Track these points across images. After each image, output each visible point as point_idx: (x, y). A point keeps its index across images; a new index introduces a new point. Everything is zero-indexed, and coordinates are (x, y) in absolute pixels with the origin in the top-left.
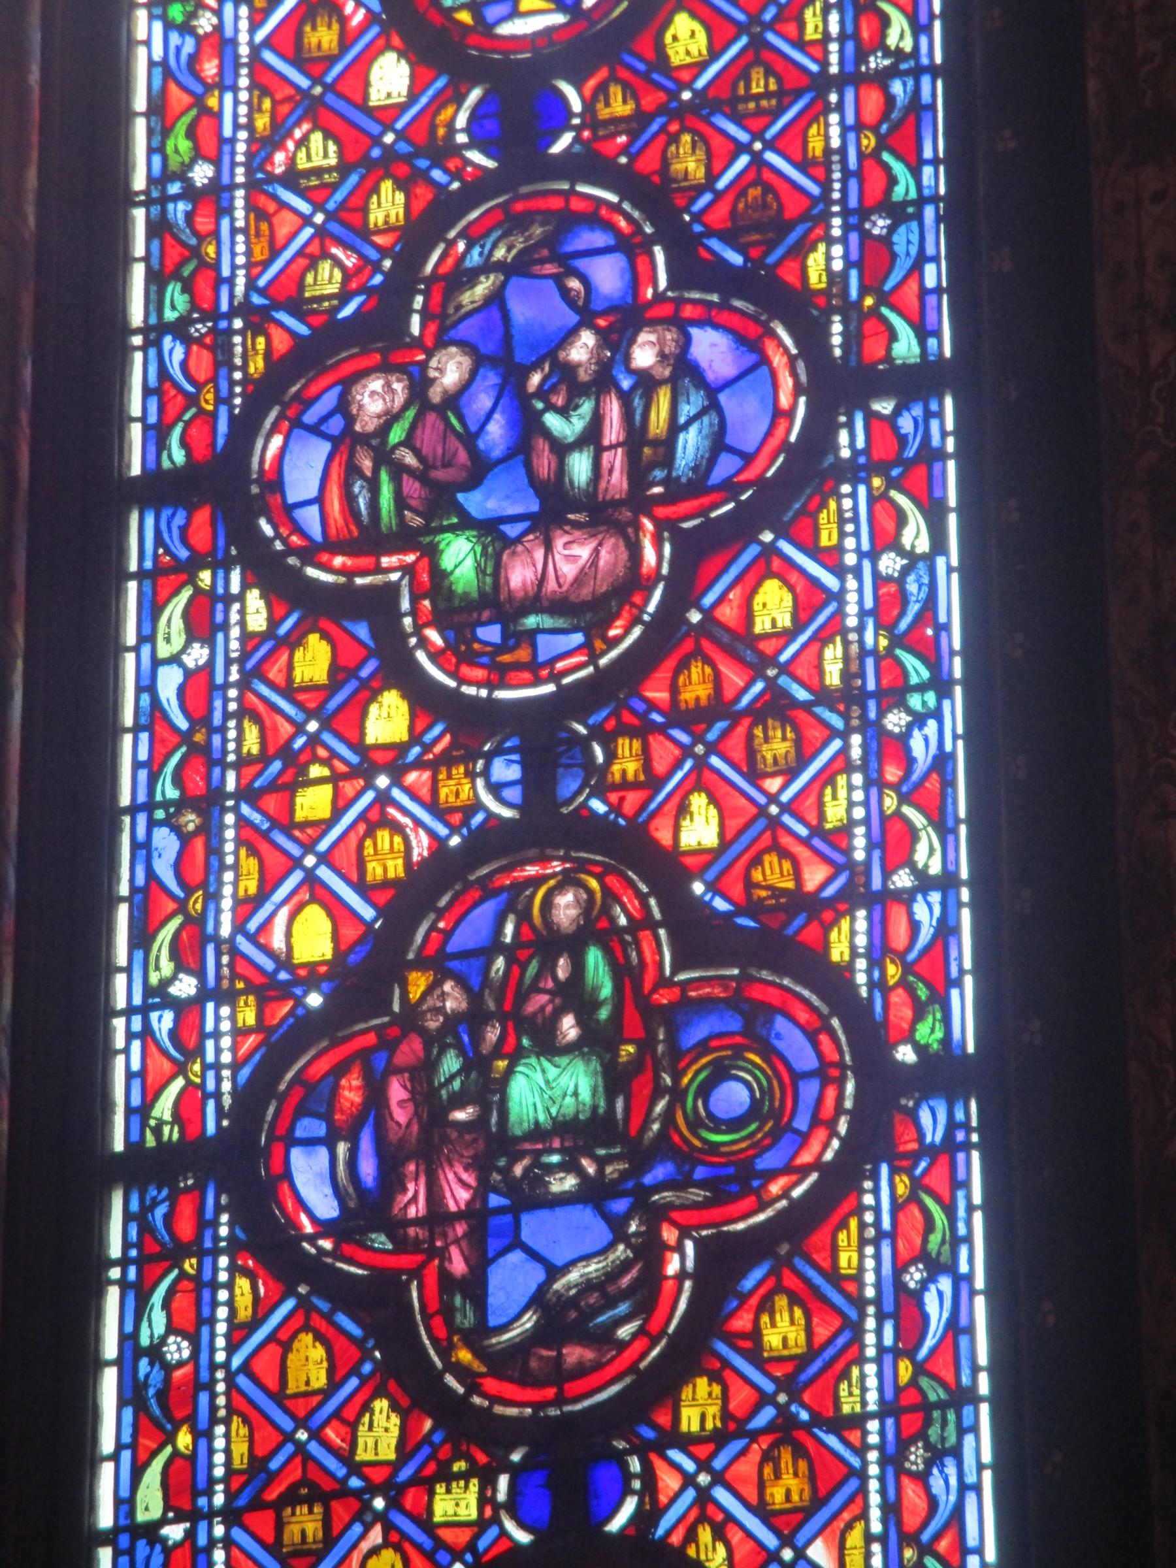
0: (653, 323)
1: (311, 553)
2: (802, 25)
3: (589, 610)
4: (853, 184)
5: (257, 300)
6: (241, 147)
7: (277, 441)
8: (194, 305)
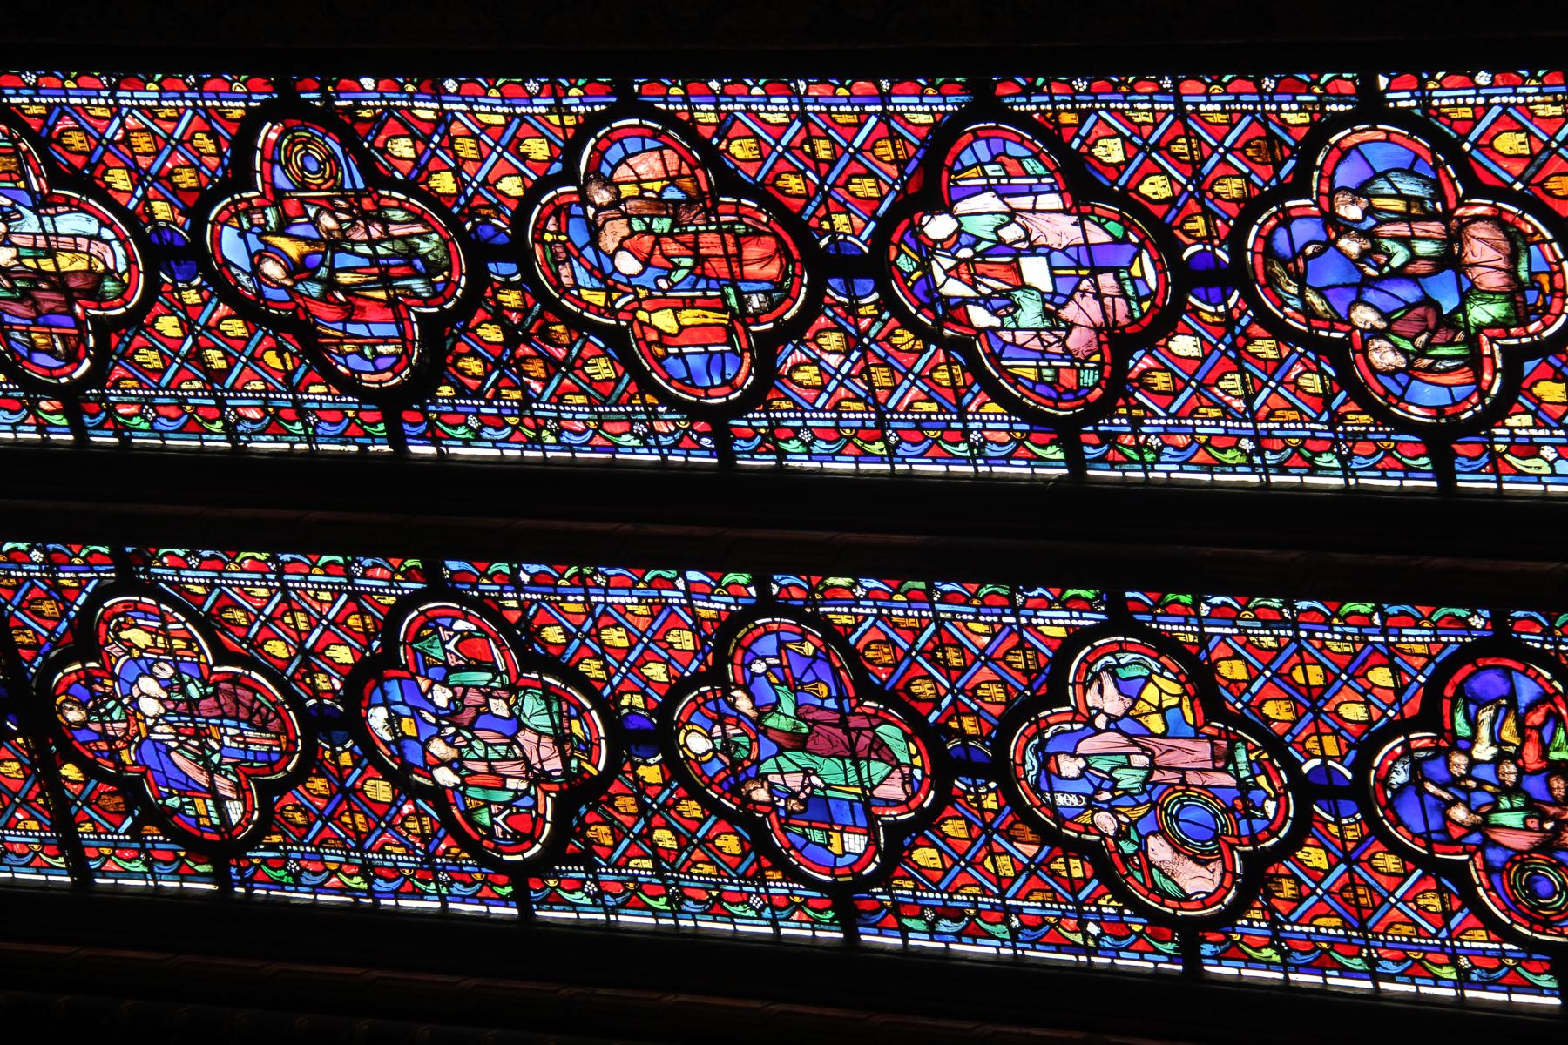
1: (1483, 394)
3: (1517, 242)
4: (1242, 98)
5: (1325, 417)
6: (1230, 424)
7: (1412, 409)
8: (1330, 451)
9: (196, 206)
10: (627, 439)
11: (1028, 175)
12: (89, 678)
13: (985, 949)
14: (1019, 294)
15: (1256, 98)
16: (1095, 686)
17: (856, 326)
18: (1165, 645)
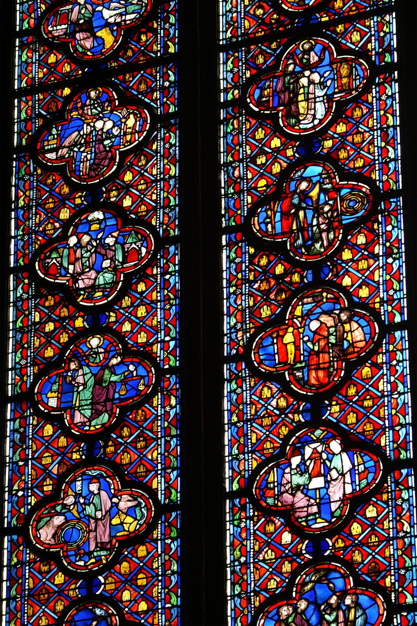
0: (350, 594)
2: (383, 525)
5: (257, 589)
6: (252, 553)
7: (262, 621)
8: (242, 590)
9: (330, 159)
10: (233, 321)
11: (359, 481)
12: (111, 101)
13: (8, 451)
14: (307, 476)
15: (396, 567)
16: (131, 499)
17: (289, 413)
18: (151, 526)
